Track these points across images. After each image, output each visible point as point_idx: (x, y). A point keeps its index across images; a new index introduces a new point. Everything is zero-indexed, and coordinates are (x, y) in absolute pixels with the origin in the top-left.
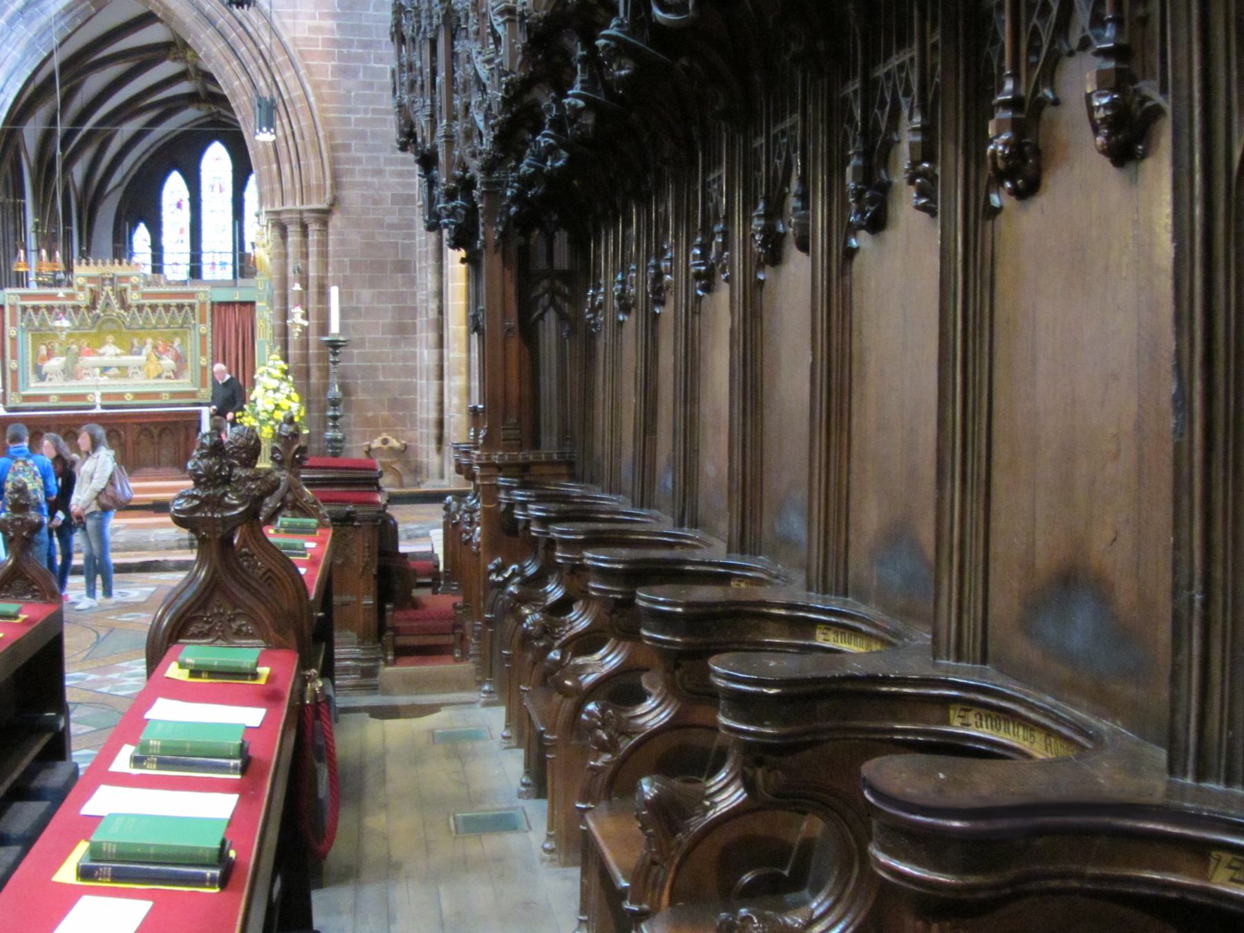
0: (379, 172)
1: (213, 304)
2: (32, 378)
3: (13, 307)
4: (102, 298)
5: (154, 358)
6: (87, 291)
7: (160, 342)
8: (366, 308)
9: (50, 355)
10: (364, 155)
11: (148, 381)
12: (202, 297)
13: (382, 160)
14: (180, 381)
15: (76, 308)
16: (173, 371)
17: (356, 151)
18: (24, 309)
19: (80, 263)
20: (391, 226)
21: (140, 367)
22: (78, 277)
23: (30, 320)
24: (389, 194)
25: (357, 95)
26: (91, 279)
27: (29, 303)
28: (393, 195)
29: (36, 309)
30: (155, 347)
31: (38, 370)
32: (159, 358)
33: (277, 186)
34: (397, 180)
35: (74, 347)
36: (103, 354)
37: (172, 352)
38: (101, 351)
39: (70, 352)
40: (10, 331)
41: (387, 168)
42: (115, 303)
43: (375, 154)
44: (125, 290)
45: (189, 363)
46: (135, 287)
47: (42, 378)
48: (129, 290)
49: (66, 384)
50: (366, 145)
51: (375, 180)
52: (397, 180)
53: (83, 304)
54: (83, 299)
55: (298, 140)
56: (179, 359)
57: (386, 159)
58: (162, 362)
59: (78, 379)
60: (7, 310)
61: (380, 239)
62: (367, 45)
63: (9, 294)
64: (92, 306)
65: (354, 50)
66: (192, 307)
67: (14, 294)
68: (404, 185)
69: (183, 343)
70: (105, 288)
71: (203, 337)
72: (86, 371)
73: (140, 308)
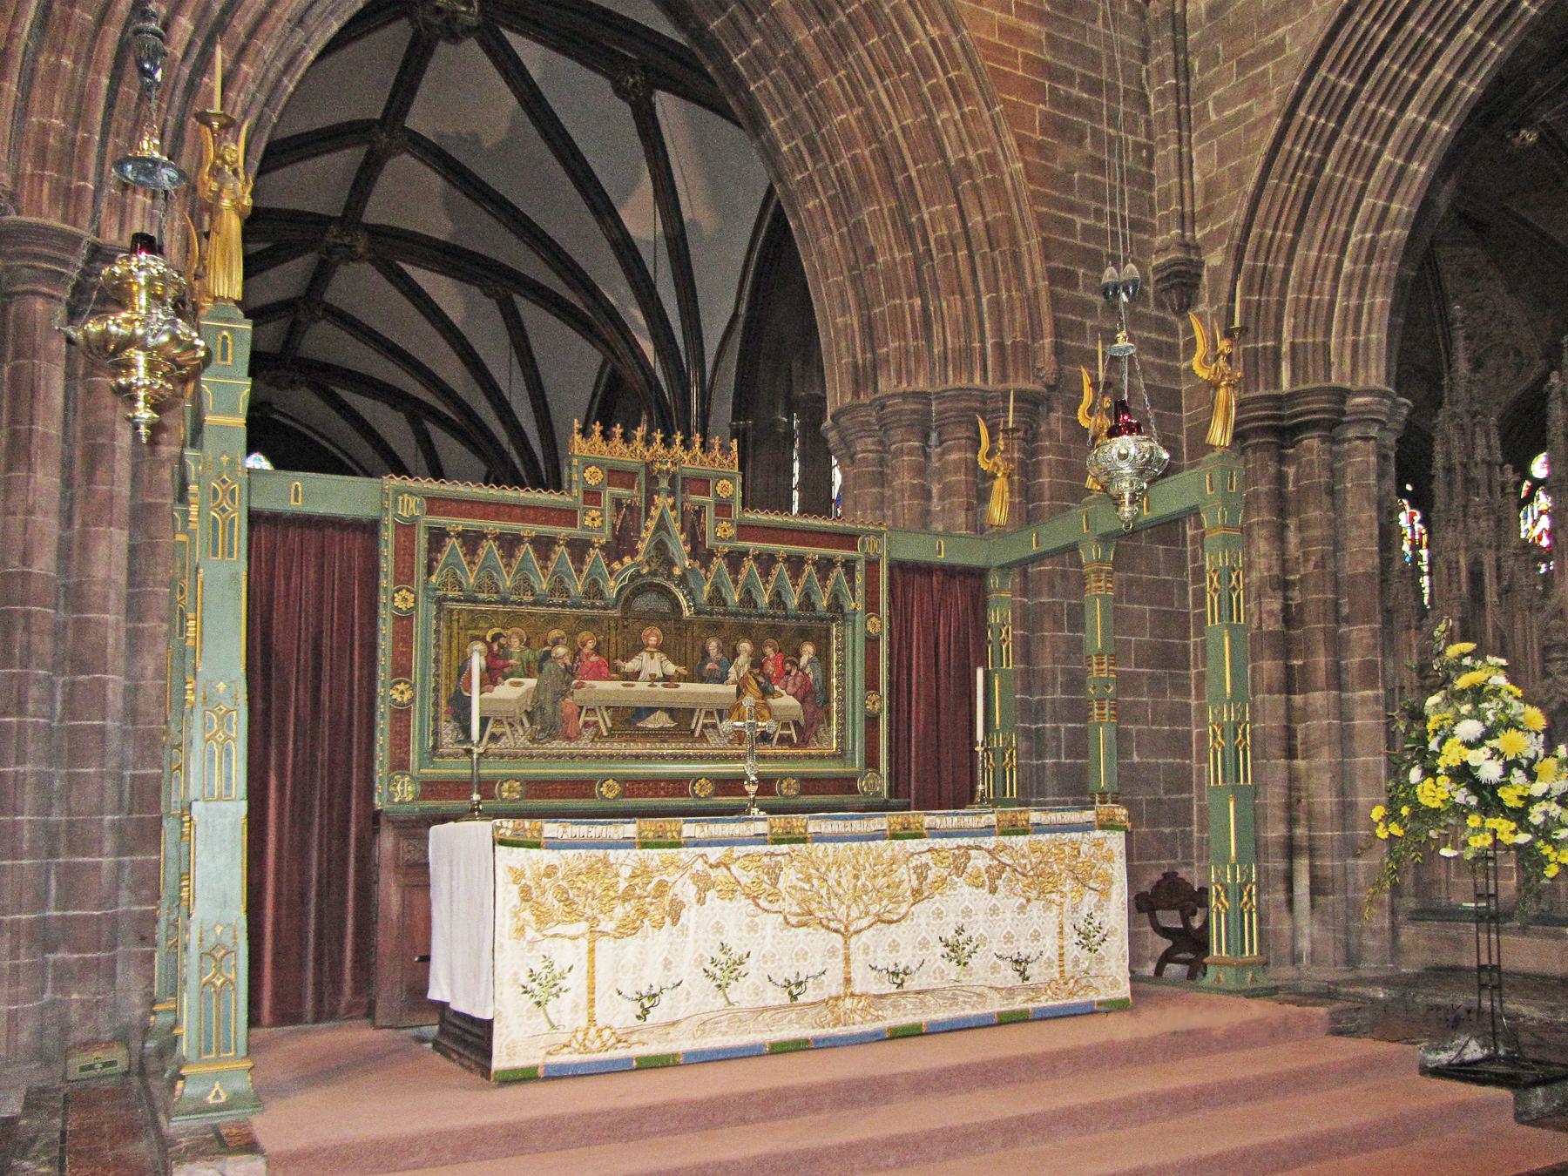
3: (406, 529)
4: (651, 524)
16: (796, 723)
19: (585, 432)
21: (720, 712)
25: (1082, 179)
30: (757, 663)
36: (635, 676)
37: (794, 680)
38: (630, 666)
39: (547, 666)
44: (699, 512)
46: (723, 508)
48: (710, 513)
49: (536, 749)
56: (815, 698)
58: (772, 702)
59: (569, 739)
60: (388, 535)
62: (1094, 87)
65: (1075, 92)
69: (822, 656)
71: (872, 642)
72: (591, 719)
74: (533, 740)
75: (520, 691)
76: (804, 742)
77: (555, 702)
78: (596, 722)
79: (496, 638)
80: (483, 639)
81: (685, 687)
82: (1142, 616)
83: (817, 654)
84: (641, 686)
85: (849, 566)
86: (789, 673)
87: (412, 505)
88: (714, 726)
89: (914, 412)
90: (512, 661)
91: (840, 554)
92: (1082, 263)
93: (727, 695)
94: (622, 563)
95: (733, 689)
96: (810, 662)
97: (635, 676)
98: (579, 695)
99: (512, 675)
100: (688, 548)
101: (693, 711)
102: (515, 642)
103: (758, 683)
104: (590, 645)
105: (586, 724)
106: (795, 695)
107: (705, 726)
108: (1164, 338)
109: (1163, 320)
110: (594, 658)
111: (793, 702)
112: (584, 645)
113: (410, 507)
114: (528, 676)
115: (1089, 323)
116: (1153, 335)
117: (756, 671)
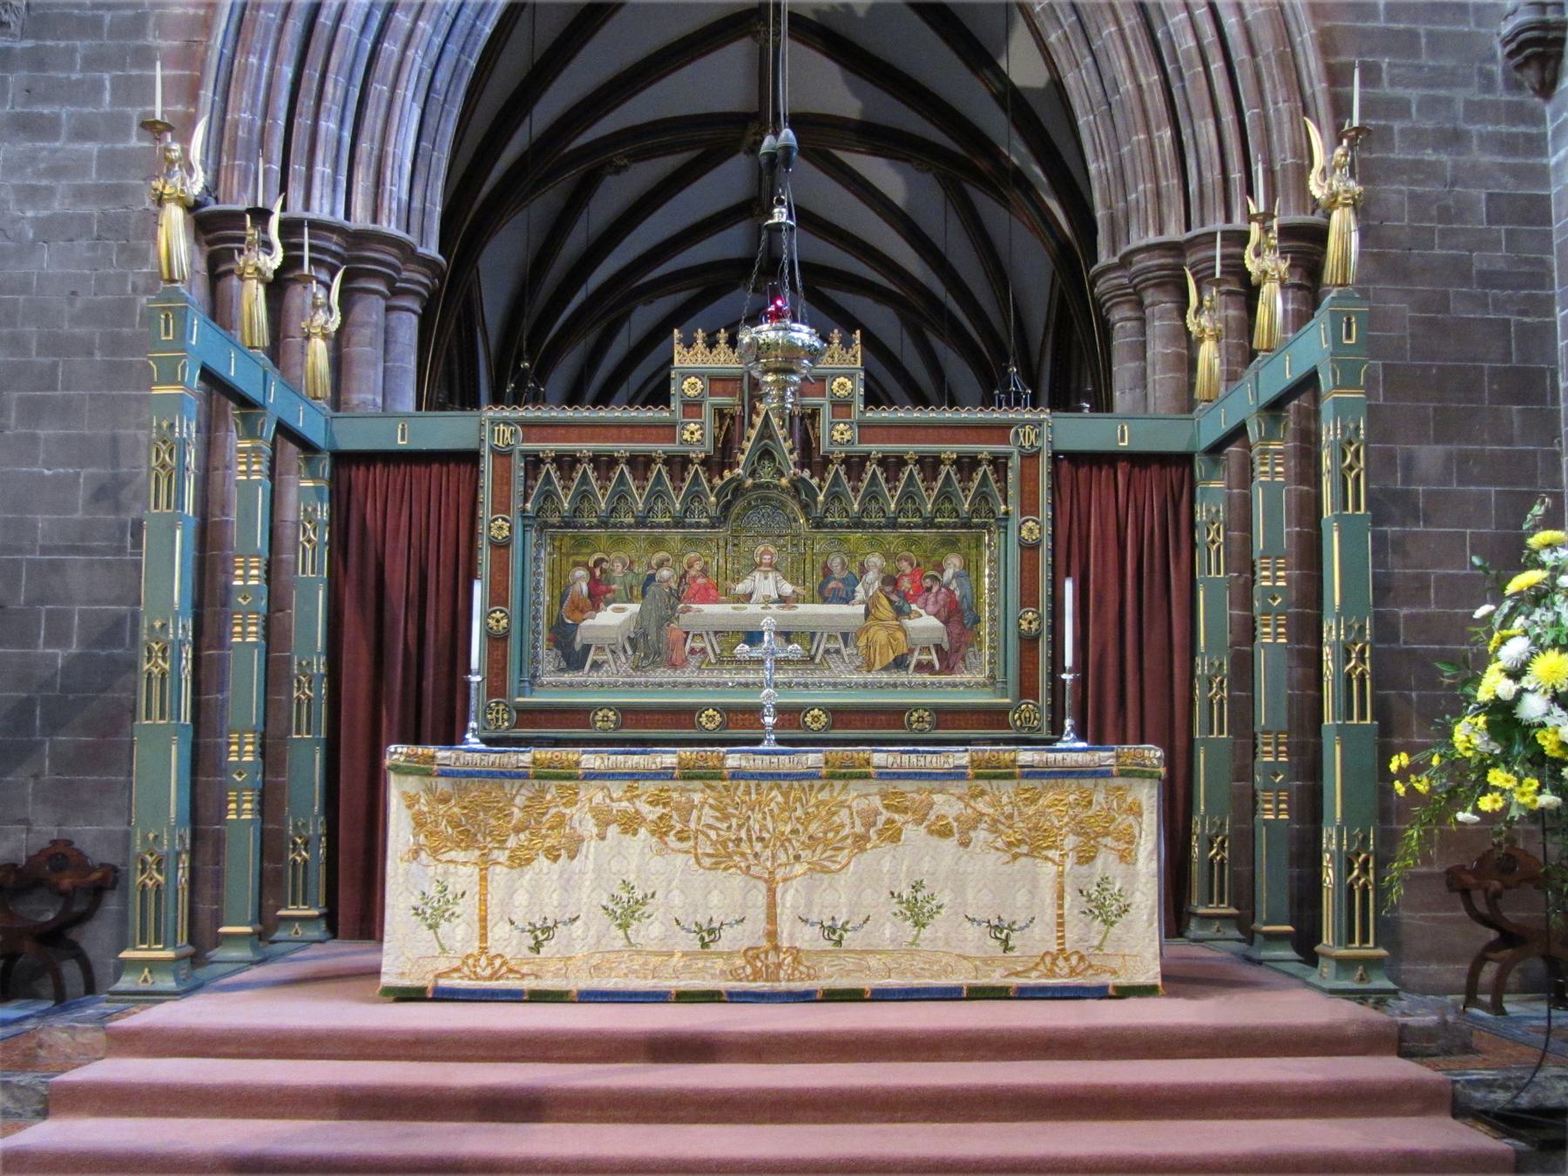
0: (1454, 139)
1: (1055, 457)
2: (548, 658)
4: (753, 434)
5: (885, 610)
6: (707, 412)
7: (905, 566)
8: (1428, 494)
9: (598, 596)
10: (1413, 94)
11: (870, 677)
12: (1028, 438)
13: (1460, 107)
14: (957, 678)
15: (677, 464)
16: (938, 648)
17: (1392, 83)
18: (534, 463)
19: (689, 343)
20: (1489, 279)
21: (845, 636)
22: (685, 376)
23: (548, 495)
24: (1481, 194)
26: (716, 381)
27: (549, 448)
28: (1490, 197)
29: (567, 463)
30: (891, 581)
31: (562, 636)
32: (900, 612)
33: (1171, 183)
34: (1500, 159)
35: (665, 573)
36: (748, 597)
37: (937, 597)
38: (741, 588)
39: (652, 588)
40: (493, 526)
41: (1474, 128)
42: (786, 446)
43: (1442, 92)
44: (814, 414)
45: (985, 629)
46: (841, 406)
47: (574, 658)
49: (639, 678)
50: (1420, 68)
51: (1444, 157)
52: (1500, 159)
53: (697, 454)
54: (696, 435)
55: (1239, 54)
56: (958, 615)
57: (1468, 103)
58: (908, 623)
59: (674, 666)
60: (487, 464)
61: (1461, 310)
63: (494, 422)
64: (720, 459)
66: (999, 464)
67: (507, 423)
68: (1517, 173)
70: (761, 407)
72: (698, 645)
73: (855, 465)
74: (636, 668)
75: (622, 617)
76: (948, 668)
77: (660, 627)
78: (703, 650)
79: (598, 563)
80: (586, 565)
81: (802, 608)
82: (1482, 501)
83: (966, 566)
84: (752, 609)
85: (999, 464)
86: (929, 589)
87: (508, 434)
88: (838, 651)
89: (1161, 267)
90: (613, 587)
91: (985, 449)
92: (1387, 51)
93: (855, 616)
94: (722, 478)
95: (861, 609)
96: (956, 576)
97: (748, 597)
98: (685, 619)
99: (614, 601)
100: (795, 456)
101: (813, 635)
102: (618, 567)
103: (891, 602)
104: (698, 566)
105: (692, 651)
106: (936, 615)
107: (827, 651)
108: (1521, 129)
109: (1520, 104)
110: (701, 581)
111: (934, 622)
112: (690, 566)
113: (505, 436)
114: (630, 601)
115: (1397, 126)
116: (1504, 128)
117: (889, 589)
